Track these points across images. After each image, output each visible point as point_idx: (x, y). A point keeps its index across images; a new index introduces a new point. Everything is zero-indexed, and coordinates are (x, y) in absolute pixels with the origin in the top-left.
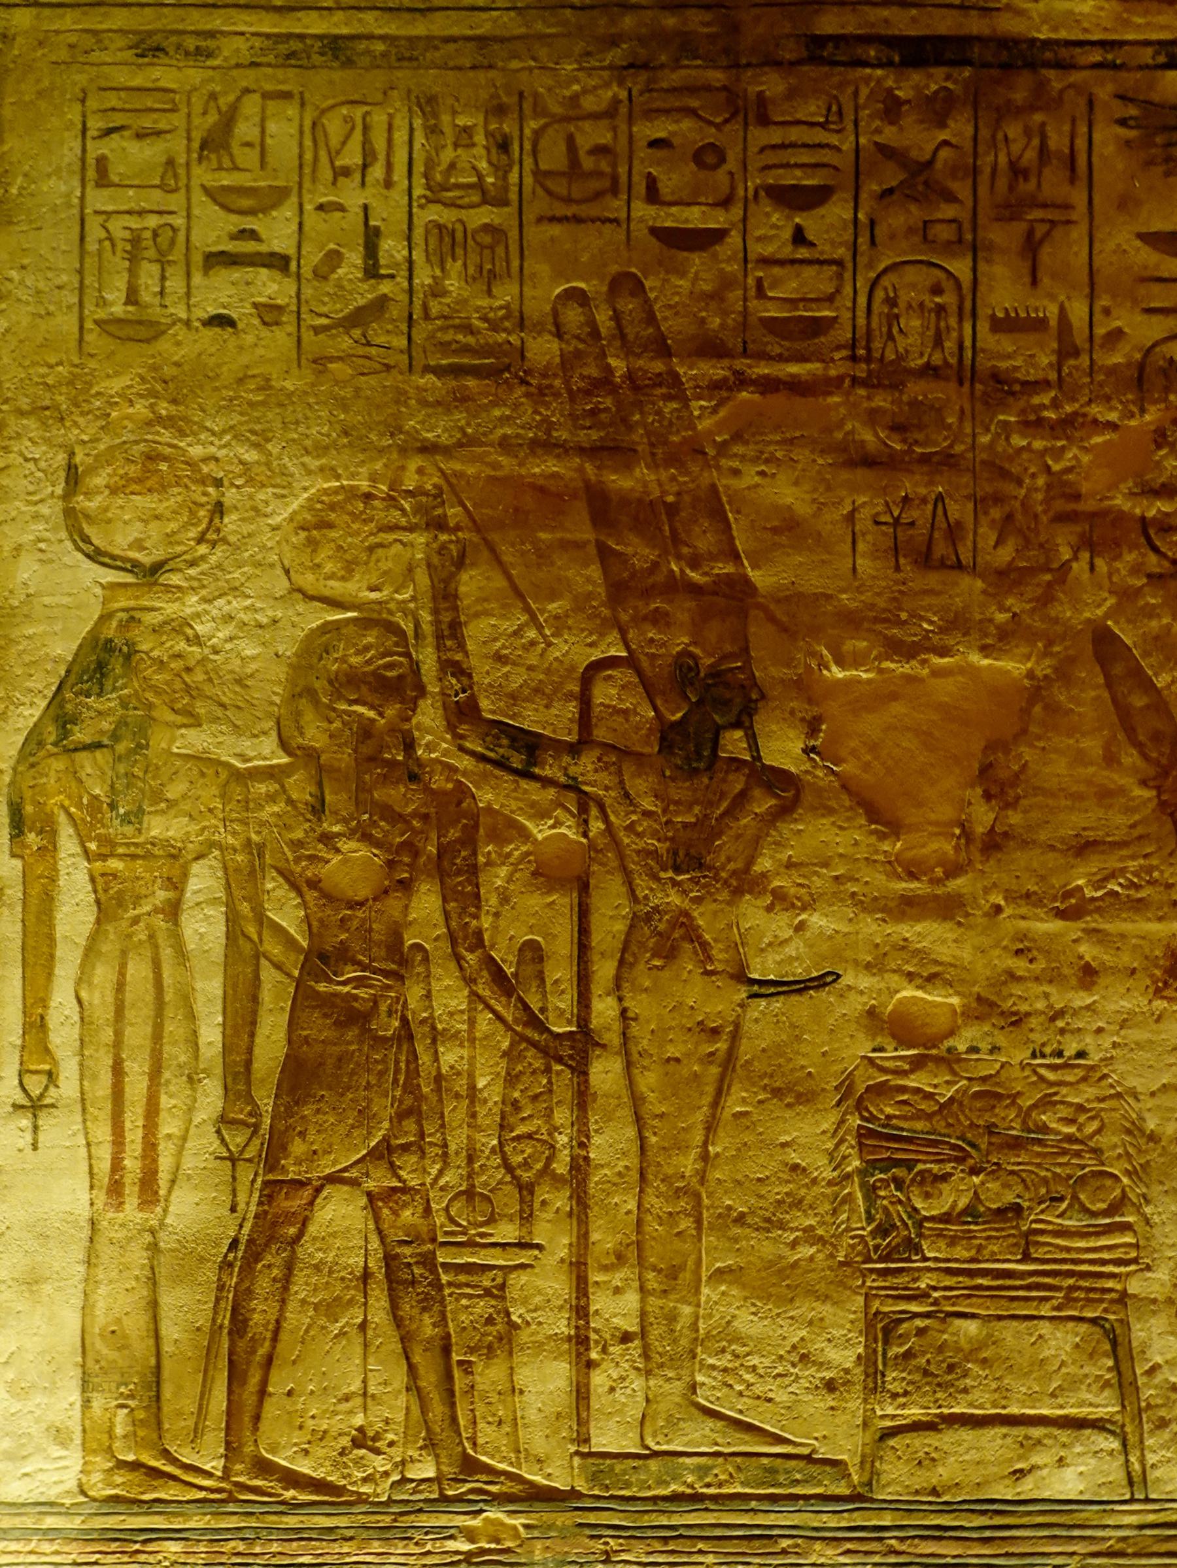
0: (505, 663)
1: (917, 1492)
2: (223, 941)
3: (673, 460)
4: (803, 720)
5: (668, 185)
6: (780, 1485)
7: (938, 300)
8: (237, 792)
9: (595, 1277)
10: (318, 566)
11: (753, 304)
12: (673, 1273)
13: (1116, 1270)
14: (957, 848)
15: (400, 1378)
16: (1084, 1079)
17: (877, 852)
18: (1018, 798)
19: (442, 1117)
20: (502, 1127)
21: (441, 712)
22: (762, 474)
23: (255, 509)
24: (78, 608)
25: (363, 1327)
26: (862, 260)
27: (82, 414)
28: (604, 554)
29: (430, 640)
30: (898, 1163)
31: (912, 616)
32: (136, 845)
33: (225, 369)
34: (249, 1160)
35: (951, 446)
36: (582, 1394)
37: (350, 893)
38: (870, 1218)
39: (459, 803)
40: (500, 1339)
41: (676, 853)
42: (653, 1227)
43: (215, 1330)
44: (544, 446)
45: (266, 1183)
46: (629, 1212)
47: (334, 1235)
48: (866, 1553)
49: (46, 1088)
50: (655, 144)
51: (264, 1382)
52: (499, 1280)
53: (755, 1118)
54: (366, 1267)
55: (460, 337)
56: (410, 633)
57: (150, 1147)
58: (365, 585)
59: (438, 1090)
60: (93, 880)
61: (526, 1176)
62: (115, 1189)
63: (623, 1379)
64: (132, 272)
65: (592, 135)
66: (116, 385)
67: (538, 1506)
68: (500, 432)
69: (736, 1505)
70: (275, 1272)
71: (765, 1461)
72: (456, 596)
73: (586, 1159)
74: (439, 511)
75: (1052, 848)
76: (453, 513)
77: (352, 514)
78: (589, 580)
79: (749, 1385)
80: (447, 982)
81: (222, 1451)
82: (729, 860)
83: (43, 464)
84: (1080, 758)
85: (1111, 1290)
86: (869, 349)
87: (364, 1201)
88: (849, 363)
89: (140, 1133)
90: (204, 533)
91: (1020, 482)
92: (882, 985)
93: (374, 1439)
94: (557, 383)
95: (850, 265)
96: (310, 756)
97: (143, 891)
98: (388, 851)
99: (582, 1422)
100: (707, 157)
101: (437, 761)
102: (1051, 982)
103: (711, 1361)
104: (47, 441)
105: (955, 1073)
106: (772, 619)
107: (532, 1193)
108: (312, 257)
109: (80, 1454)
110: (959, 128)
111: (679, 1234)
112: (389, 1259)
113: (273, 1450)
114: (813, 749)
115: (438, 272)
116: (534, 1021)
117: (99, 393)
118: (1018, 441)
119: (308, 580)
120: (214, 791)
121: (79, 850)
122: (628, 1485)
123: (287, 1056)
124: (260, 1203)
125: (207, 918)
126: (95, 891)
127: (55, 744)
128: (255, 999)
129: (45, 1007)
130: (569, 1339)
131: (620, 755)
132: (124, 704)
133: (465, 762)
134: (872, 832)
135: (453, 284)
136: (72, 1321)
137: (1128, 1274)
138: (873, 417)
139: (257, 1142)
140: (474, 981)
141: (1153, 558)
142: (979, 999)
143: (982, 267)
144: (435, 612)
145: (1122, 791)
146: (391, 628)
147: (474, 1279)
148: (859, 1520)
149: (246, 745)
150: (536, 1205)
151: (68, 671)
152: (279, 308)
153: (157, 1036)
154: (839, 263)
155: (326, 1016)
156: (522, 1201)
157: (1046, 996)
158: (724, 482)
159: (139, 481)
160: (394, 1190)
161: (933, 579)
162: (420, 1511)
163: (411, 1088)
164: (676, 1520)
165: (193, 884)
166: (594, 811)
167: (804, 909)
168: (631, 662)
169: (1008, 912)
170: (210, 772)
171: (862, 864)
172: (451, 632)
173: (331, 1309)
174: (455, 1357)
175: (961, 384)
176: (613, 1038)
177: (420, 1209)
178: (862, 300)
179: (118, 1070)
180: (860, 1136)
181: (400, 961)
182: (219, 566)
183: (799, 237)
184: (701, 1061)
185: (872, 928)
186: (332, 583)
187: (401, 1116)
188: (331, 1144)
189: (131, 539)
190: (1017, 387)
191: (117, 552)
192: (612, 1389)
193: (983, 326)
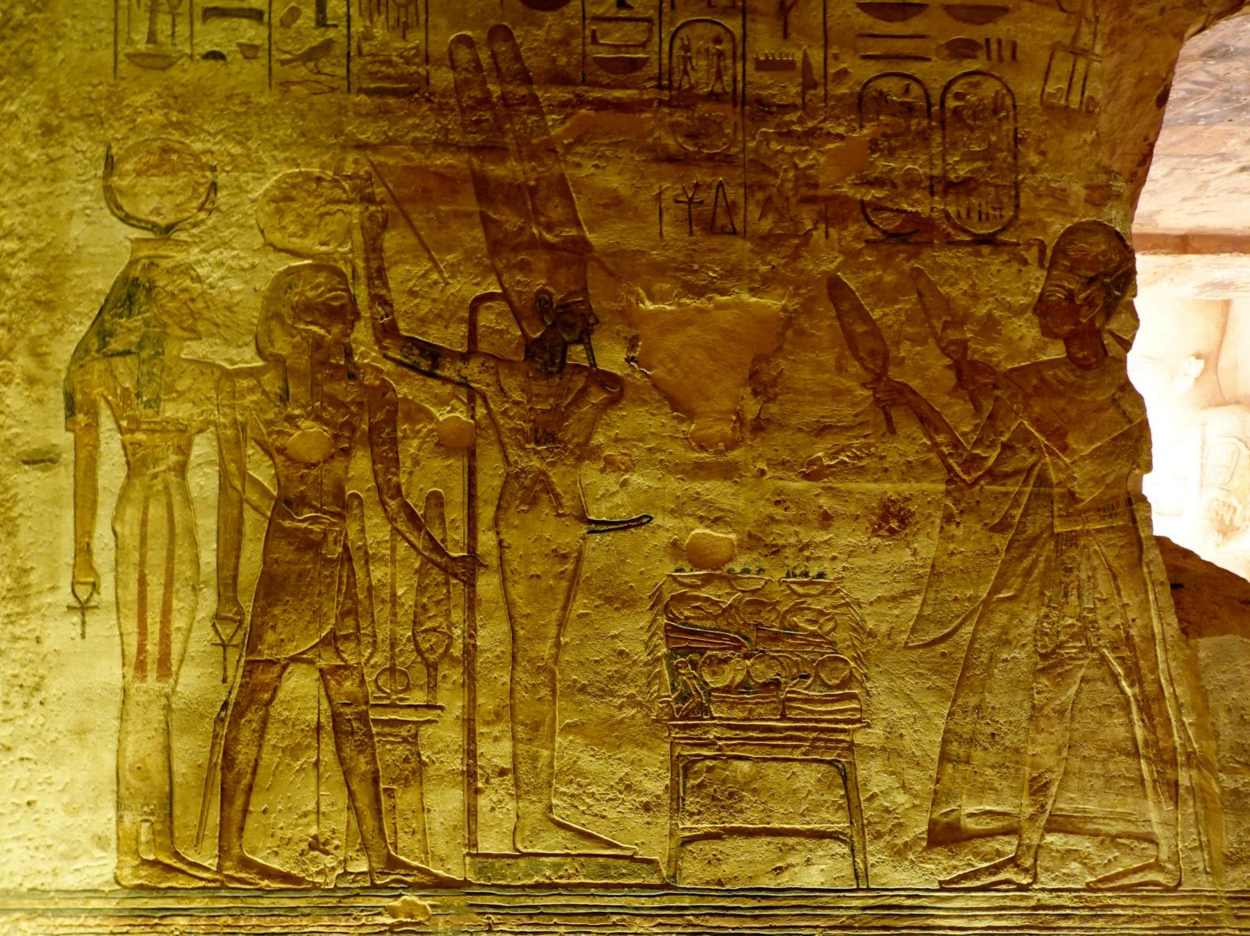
0: (416, 297)
1: (708, 883)
2: (217, 491)
3: (533, 156)
4: (625, 338)
6: (612, 877)
8: (227, 386)
9: (481, 729)
10: (284, 228)
11: (589, 48)
12: (536, 727)
13: (846, 727)
14: (734, 430)
15: (343, 801)
16: (823, 593)
17: (677, 431)
18: (776, 395)
21: (371, 330)
22: (596, 166)
23: (239, 187)
24: (114, 255)
25: (317, 764)
26: (665, 19)
27: (117, 119)
28: (486, 221)
29: (363, 280)
30: (693, 650)
31: (701, 267)
32: (155, 423)
33: (218, 89)
34: (236, 646)
35: (728, 149)
36: (471, 812)
37: (307, 458)
38: (674, 689)
39: (384, 394)
40: (414, 773)
41: (536, 431)
42: (521, 694)
43: (212, 766)
44: (442, 145)
45: (248, 662)
46: (504, 684)
47: (296, 699)
48: (672, 925)
49: (91, 594)
52: (413, 731)
54: (319, 722)
55: (384, 69)
56: (349, 276)
57: (165, 638)
58: (317, 241)
59: (370, 596)
60: (124, 447)
61: (432, 657)
62: (141, 666)
63: (500, 801)
64: (152, 21)
66: (140, 100)
67: (441, 892)
68: (412, 135)
70: (254, 725)
71: (601, 860)
72: (381, 250)
73: (474, 646)
74: (370, 190)
75: (800, 430)
76: (380, 191)
77: (308, 191)
78: (474, 239)
79: (589, 806)
81: (216, 852)
82: (574, 436)
83: (88, 155)
84: (819, 367)
85: (843, 741)
86: (670, 81)
87: (317, 675)
88: (657, 91)
89: (158, 626)
91: (776, 175)
92: (682, 525)
93: (324, 844)
94: (452, 101)
95: (657, 22)
96: (277, 361)
97: (161, 455)
98: (334, 427)
102: (799, 524)
103: (562, 789)
104: (92, 138)
105: (733, 587)
106: (602, 266)
107: (436, 670)
108: (279, 12)
109: (115, 855)
111: (540, 699)
112: (336, 717)
113: (253, 852)
114: (633, 359)
115: (368, 23)
116: (437, 548)
117: (128, 106)
118: (775, 146)
119: (276, 237)
120: (210, 385)
121: (114, 426)
122: (504, 877)
123: (263, 572)
124: (244, 676)
125: (206, 474)
126: (126, 455)
127: (98, 351)
128: (240, 532)
129: (90, 537)
130: (463, 773)
131: (497, 362)
132: (147, 323)
133: (388, 366)
134: (674, 418)
135: (378, 31)
136: (109, 760)
137: (854, 730)
138: (674, 128)
139: (241, 633)
140: (395, 520)
141: (869, 229)
142: (750, 535)
143: (749, 25)
144: (367, 260)
145: (849, 391)
148: (666, 902)
149: (233, 353)
150: (439, 678)
151: (107, 300)
152: (256, 47)
153: (170, 558)
154: (649, 20)
155: (290, 544)
156: (429, 676)
157: (797, 533)
158: (569, 172)
159: (156, 167)
160: (338, 667)
161: (716, 241)
162: (358, 895)
163: (350, 595)
164: (538, 902)
165: (196, 451)
166: (479, 401)
167: (627, 471)
168: (505, 296)
169: (769, 474)
170: (208, 371)
171: (667, 440)
172: (378, 275)
173: (294, 751)
174: (382, 786)
175: (735, 106)
176: (493, 561)
177: (357, 681)
178: (666, 46)
179: (142, 582)
180: (666, 631)
181: (342, 505)
182: (214, 227)
184: (555, 577)
185: (674, 485)
187: (344, 615)
188: (294, 634)
189: (151, 208)
190: (774, 109)
191: (142, 216)
192: (493, 809)
193: (750, 66)
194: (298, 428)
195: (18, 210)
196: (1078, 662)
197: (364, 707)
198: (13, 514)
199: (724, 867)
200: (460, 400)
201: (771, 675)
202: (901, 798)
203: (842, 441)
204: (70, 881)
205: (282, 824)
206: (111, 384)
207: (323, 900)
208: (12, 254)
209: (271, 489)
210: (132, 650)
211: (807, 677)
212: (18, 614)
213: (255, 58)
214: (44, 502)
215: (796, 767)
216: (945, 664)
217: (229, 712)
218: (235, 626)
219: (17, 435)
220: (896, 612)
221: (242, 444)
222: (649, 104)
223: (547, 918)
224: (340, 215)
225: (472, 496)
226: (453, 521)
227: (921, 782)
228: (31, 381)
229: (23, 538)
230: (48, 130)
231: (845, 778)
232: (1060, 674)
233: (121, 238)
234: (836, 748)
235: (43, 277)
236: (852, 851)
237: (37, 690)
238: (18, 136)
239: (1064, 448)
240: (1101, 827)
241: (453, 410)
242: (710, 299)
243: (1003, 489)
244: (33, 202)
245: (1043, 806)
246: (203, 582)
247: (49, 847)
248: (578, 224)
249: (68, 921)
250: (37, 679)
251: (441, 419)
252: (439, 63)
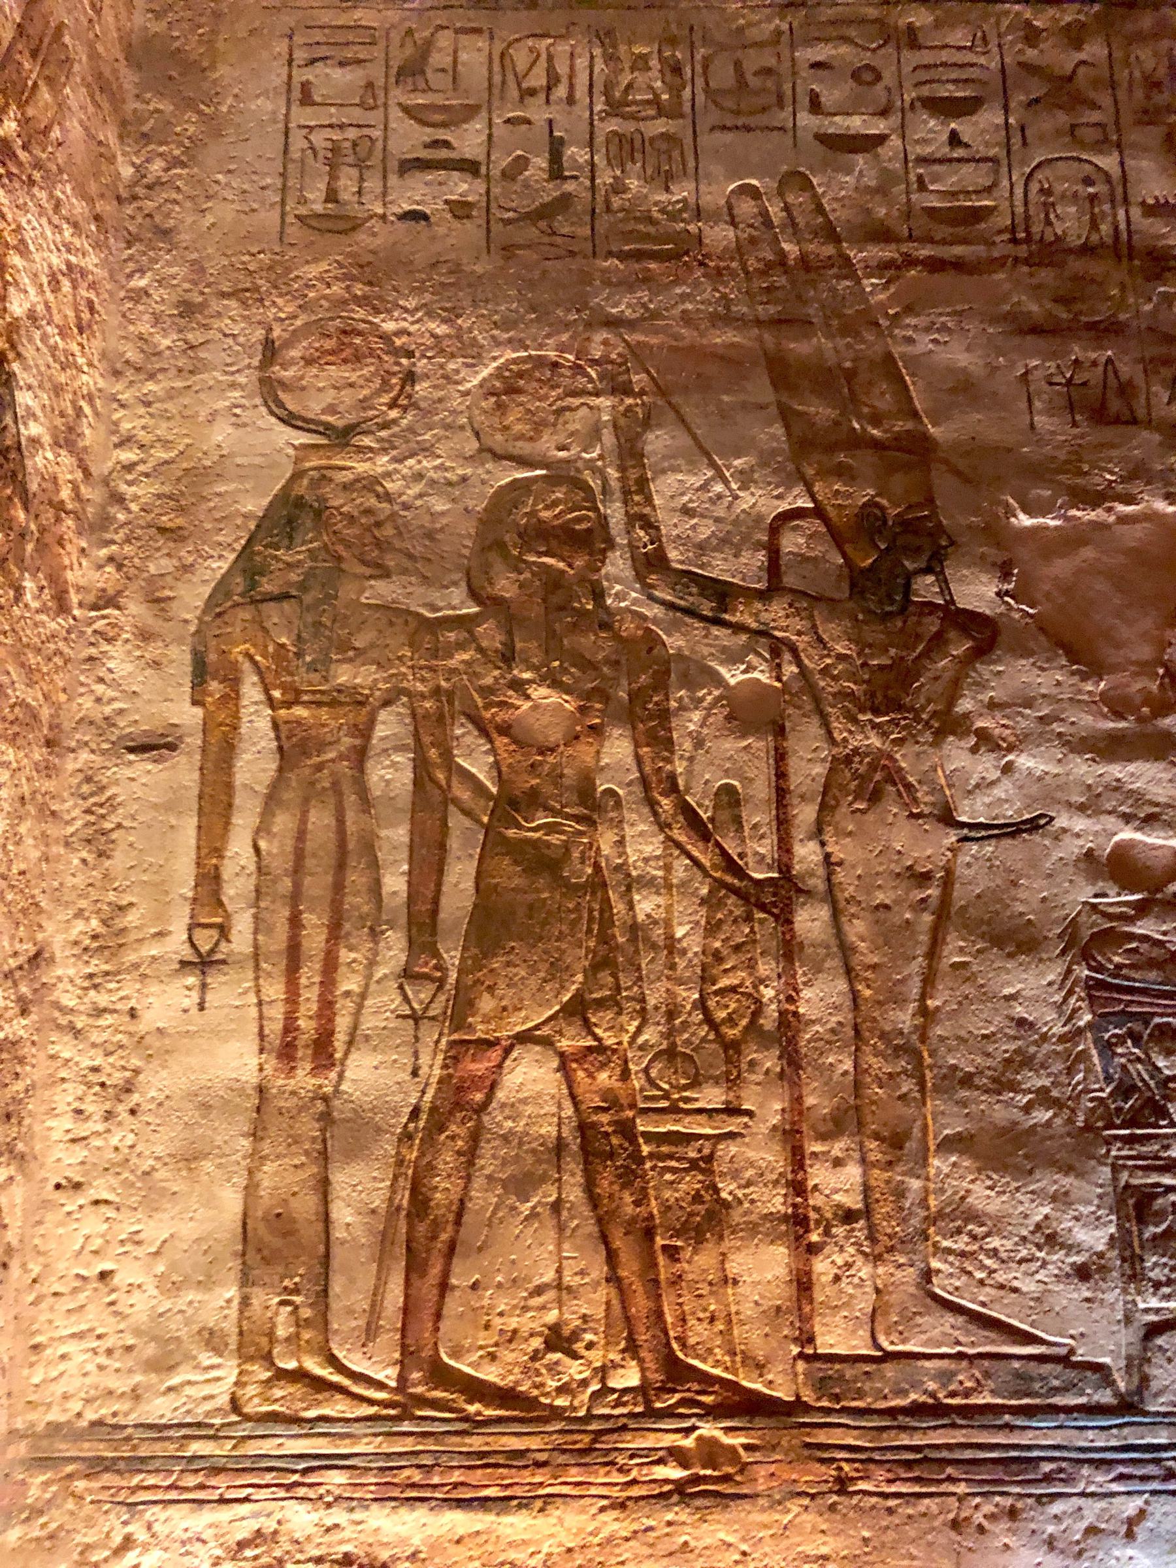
0: (693, 517)
2: (410, 787)
3: (848, 329)
4: (994, 564)
5: (830, 96)
6: (1036, 1395)
7: (1091, 190)
8: (427, 641)
10: (506, 428)
15: (599, 1270)
17: (1080, 692)
19: (639, 969)
20: (702, 978)
22: (934, 341)
23: (446, 377)
24: (269, 467)
25: (556, 1207)
27: (281, 295)
28: (786, 415)
29: (618, 495)
34: (433, 1018)
36: (803, 1284)
37: (541, 738)
38: (1108, 1079)
39: (650, 650)
41: (873, 695)
43: (393, 1210)
45: (452, 1044)
46: (845, 1073)
47: (524, 1101)
49: (217, 944)
50: (817, 65)
51: (446, 1274)
52: (706, 1151)
53: (975, 968)
55: (641, 227)
56: (597, 490)
57: (327, 1007)
59: (633, 940)
61: (731, 1033)
63: (848, 1265)
64: (333, 177)
65: (754, 61)
67: (759, 1422)
68: (681, 307)
69: (988, 1420)
71: (1016, 1365)
76: (638, 379)
78: (774, 437)
80: (642, 827)
81: (397, 1355)
82: (929, 701)
83: (241, 339)
86: (1028, 233)
89: (316, 990)
90: (395, 399)
92: (1098, 827)
95: (1005, 162)
97: (329, 738)
98: (579, 697)
99: (806, 1319)
100: (865, 76)
101: (627, 609)
103: (945, 1244)
107: (739, 1053)
110: (1094, 50)
112: (584, 1128)
113: (456, 1354)
114: (1007, 593)
119: (498, 440)
120: (403, 639)
121: (262, 697)
122: (860, 1394)
123: (475, 906)
124: (445, 1066)
125: (394, 764)
126: (278, 738)
127: (241, 595)
128: (443, 846)
129: (221, 857)
130: (785, 1218)
131: (808, 601)
133: (653, 611)
134: (1073, 673)
136: (231, 1201)
139: (442, 998)
140: (669, 826)
144: (622, 469)
146: (579, 484)
147: (680, 1150)
149: (435, 596)
150: (744, 1066)
153: (338, 887)
154: (994, 160)
158: (897, 350)
159: (332, 353)
160: (589, 1048)
161: (1109, 433)
162: (624, 1428)
163: (605, 939)
165: (380, 731)
166: (787, 656)
167: (1010, 749)
168: (818, 512)
170: (400, 621)
172: (638, 488)
173: (521, 1185)
174: (660, 1241)
176: (817, 883)
177: (618, 1071)
178: (1019, 191)
179: (295, 922)
180: (1088, 988)
181: (592, 806)
182: (411, 429)
183: (955, 139)
184: (912, 907)
185: (1083, 769)
186: (519, 444)
187: (596, 967)
191: (311, 416)
192: (837, 1279)
194: (528, 697)
195: (142, 410)
197: (630, 1114)
198: (108, 826)
200: (760, 655)
204: (160, 1409)
205: (502, 1307)
206: (260, 641)
207: (570, 1438)
208: (129, 467)
209: (488, 784)
210: (275, 1027)
212: (107, 973)
213: (468, 217)
214: (155, 806)
217: (421, 1124)
218: (432, 987)
219: (121, 712)
221: (448, 721)
222: (1000, 263)
223: (935, 1467)
224: (584, 411)
225: (781, 794)
226: (755, 827)
228: (145, 636)
229: (119, 861)
230: (187, 309)
233: (281, 443)
235: (170, 497)
237: (128, 1091)
238: (146, 317)
241: (750, 668)
242: (1110, 510)
244: (161, 401)
246: (387, 922)
247: (129, 1349)
248: (915, 415)
249: (151, 1481)
250: (128, 1074)
251: (732, 682)
252: (713, 217)
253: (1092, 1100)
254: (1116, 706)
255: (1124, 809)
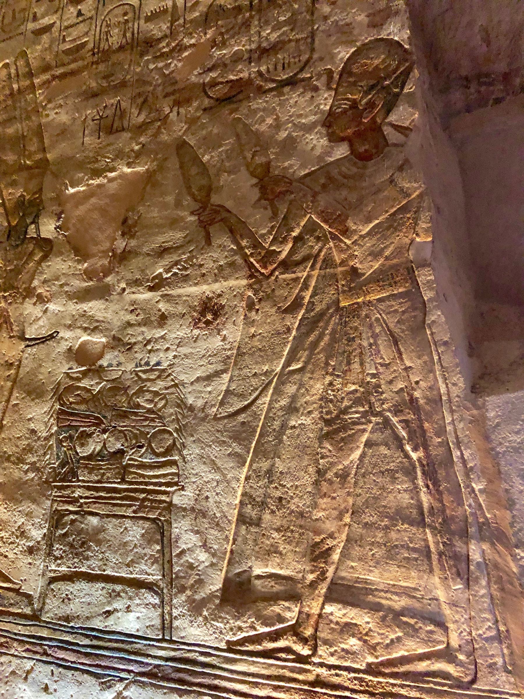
1: (60, 619)
6: (5, 606)
16: (159, 377)
38: (58, 458)
53: (20, 406)
75: (148, 255)
85: (164, 501)
102: (145, 325)
105: (100, 378)
137: (174, 493)
142: (114, 338)
157: (143, 333)
167: (47, 302)
180: (58, 414)
185: (74, 308)
196: (364, 427)
199: (72, 606)
201: (119, 446)
202: (203, 556)
203: (175, 258)
211: (141, 447)
215: (128, 523)
216: (244, 432)
220: (209, 389)
227: (222, 541)
231: (162, 535)
232: (343, 439)
234: (158, 508)
236: (162, 602)
239: (346, 232)
240: (384, 602)
243: (293, 276)
245: (324, 573)
253: (50, 468)
254: (89, 274)
255: (85, 325)
